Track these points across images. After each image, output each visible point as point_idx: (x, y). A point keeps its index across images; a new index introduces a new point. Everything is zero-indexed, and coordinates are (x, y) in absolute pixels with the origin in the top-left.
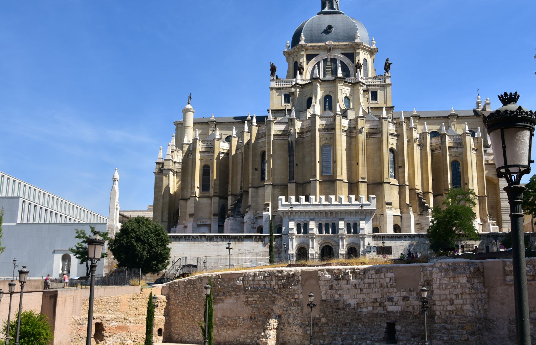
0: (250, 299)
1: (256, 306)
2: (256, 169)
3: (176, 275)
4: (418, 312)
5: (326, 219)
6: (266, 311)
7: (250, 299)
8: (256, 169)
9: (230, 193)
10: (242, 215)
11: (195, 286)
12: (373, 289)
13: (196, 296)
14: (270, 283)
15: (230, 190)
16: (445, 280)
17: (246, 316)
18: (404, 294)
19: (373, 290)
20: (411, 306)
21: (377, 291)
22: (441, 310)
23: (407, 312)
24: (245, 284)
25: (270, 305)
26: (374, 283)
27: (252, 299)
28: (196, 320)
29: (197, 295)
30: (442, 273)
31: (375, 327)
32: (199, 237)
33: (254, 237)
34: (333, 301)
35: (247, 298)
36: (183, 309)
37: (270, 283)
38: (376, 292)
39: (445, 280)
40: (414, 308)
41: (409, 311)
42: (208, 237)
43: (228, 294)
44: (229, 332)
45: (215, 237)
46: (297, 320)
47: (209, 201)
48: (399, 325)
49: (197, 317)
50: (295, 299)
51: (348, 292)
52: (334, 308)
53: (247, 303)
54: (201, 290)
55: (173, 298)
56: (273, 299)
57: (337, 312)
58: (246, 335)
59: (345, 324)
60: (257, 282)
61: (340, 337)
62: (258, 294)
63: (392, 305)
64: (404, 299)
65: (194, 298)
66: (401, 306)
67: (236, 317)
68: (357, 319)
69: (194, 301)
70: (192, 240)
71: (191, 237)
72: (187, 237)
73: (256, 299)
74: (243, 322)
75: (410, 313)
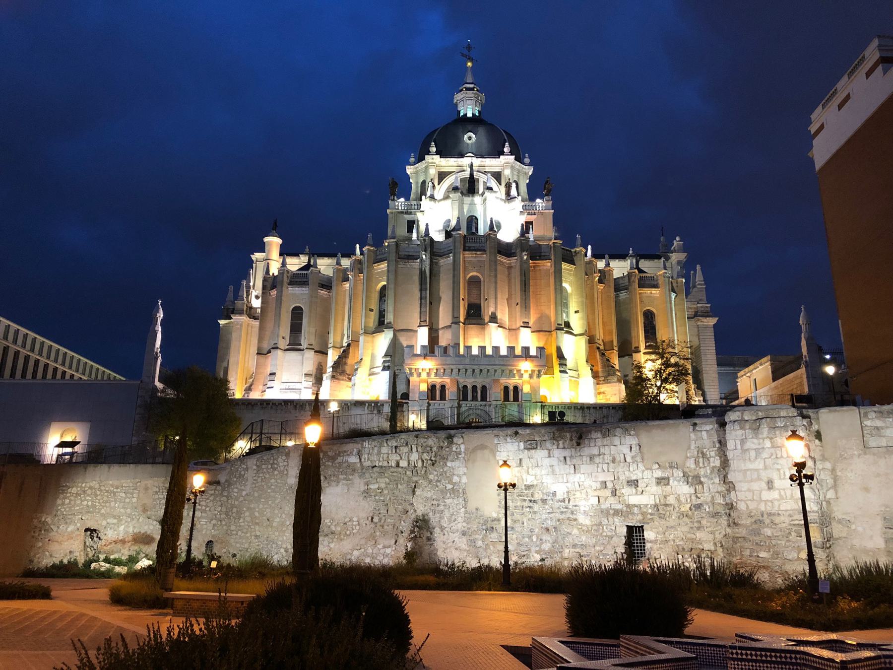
0: (372, 487)
1: (382, 498)
2: (371, 310)
3: (244, 452)
4: (689, 506)
5: (473, 380)
6: (400, 507)
7: (372, 487)
8: (371, 310)
9: (330, 346)
10: (349, 375)
11: (276, 466)
12: (598, 464)
13: (278, 483)
14: (408, 458)
15: (331, 340)
16: (753, 443)
17: (363, 515)
18: (659, 474)
19: (598, 467)
20: (672, 494)
21: (606, 469)
22: (748, 500)
23: (666, 505)
24: (363, 460)
25: (407, 497)
26: (599, 455)
27: (376, 486)
28: (275, 524)
29: (279, 481)
30: (745, 430)
31: (604, 534)
32: (283, 404)
33: (367, 404)
34: (523, 487)
35: (367, 484)
36: (252, 506)
37: (408, 458)
38: (604, 471)
39: (753, 443)
40: (678, 500)
41: (671, 505)
42: (297, 404)
43: (332, 479)
44: (332, 545)
45: (307, 404)
46: (456, 522)
47: (300, 358)
48: (652, 530)
49: (277, 520)
50: (454, 484)
51: (550, 470)
52: (525, 500)
53: (367, 493)
54: (286, 472)
55: (237, 488)
56: (414, 485)
57: (530, 507)
58: (363, 550)
59: (547, 530)
60: (385, 456)
61: (537, 552)
62: (386, 477)
63: (636, 494)
64: (661, 483)
65: (272, 487)
66: (655, 495)
67: (345, 518)
68: (568, 519)
69: (273, 492)
70: (272, 408)
71: (271, 404)
72: (265, 404)
73: (383, 486)
74: (358, 527)
75: (672, 509)
